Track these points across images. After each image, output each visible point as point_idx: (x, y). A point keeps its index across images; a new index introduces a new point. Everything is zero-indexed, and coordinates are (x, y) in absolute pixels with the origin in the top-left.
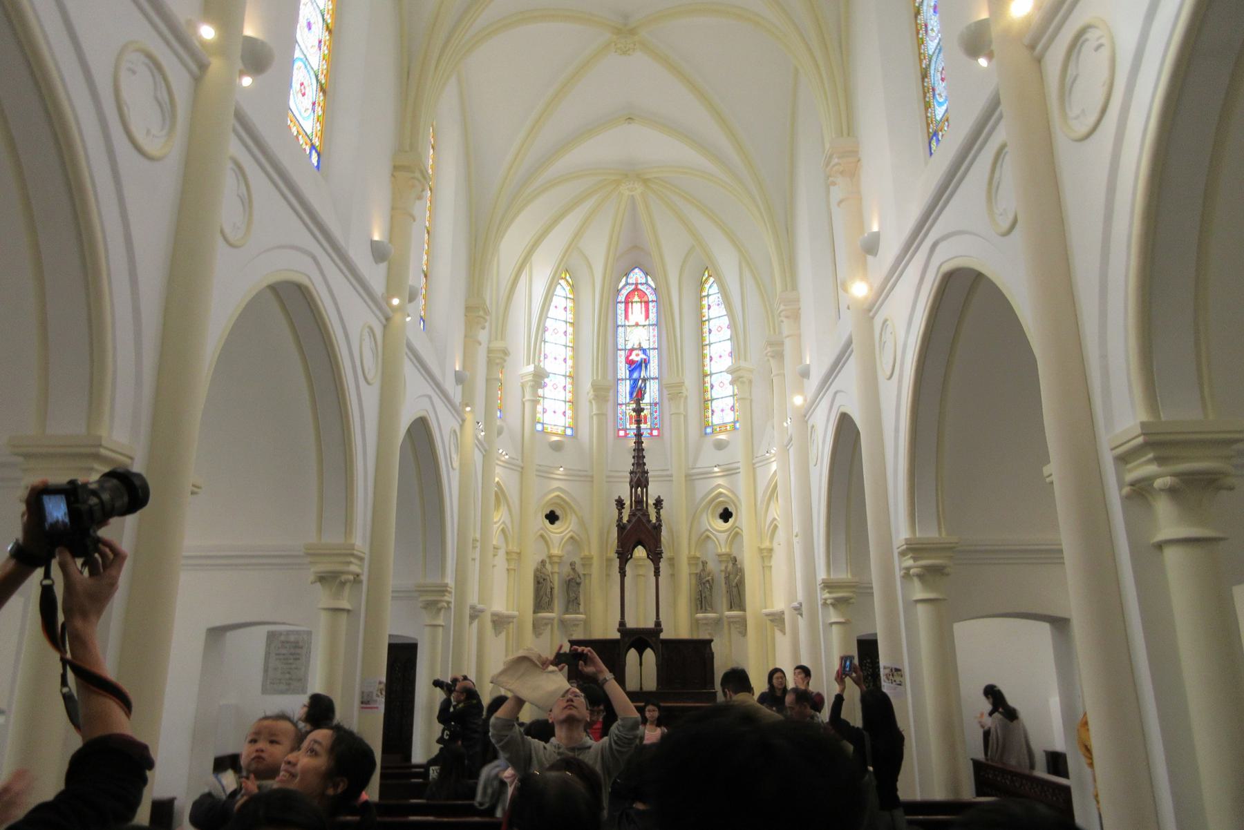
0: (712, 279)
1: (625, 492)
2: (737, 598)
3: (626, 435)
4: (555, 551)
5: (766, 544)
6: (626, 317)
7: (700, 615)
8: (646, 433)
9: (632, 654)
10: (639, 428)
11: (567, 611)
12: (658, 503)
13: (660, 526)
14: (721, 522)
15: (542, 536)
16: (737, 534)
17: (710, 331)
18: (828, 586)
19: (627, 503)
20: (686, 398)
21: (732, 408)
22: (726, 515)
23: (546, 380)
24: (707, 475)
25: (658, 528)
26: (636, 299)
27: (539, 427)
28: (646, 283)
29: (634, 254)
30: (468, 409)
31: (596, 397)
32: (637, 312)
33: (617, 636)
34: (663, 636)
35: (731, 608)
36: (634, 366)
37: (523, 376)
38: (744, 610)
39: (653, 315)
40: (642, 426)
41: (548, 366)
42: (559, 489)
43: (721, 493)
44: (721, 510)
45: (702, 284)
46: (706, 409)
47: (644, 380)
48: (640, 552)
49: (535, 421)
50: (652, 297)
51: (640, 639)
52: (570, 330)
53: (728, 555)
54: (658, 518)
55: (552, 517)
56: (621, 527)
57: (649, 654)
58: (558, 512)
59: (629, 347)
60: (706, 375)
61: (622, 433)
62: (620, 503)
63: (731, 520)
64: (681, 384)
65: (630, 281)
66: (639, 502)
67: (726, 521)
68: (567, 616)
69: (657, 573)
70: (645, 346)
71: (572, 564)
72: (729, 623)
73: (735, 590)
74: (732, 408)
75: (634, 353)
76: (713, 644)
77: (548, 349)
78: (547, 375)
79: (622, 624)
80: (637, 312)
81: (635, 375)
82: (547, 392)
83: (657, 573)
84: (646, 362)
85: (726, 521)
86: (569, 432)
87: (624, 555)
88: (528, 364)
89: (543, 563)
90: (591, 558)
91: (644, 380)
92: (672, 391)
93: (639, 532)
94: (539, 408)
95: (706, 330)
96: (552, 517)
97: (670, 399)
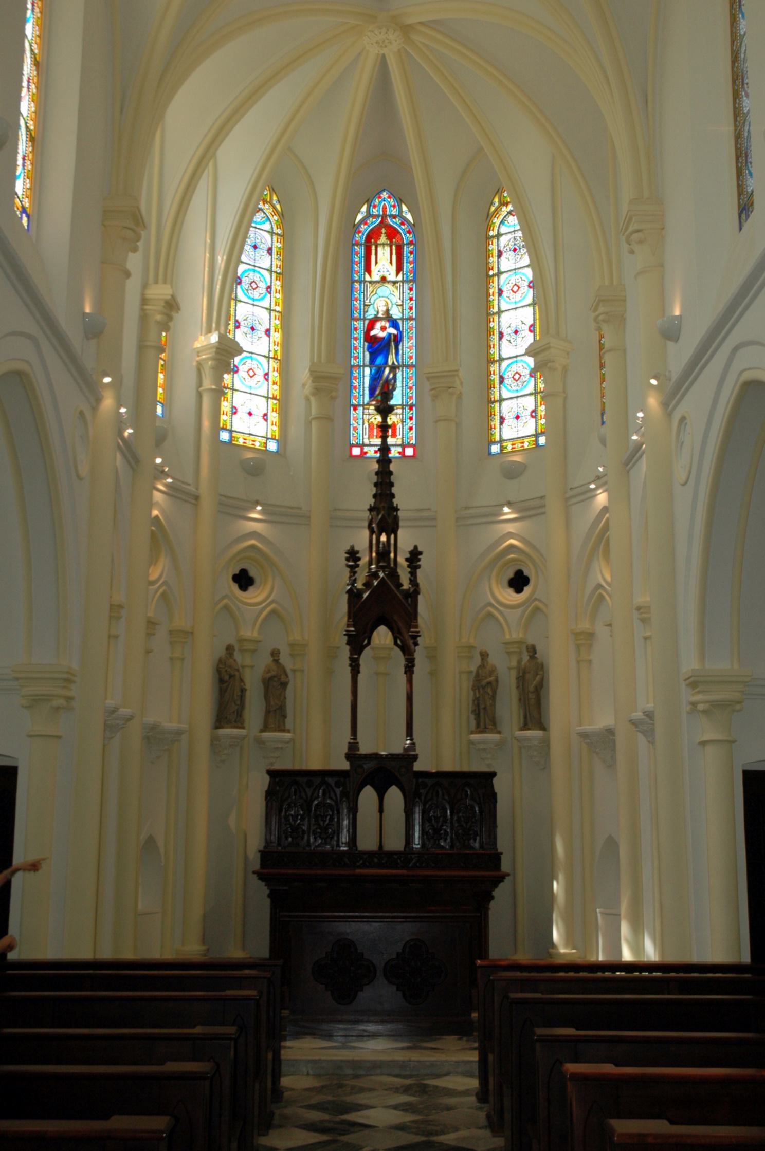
0: (505, 210)
1: (361, 539)
2: (534, 712)
3: (363, 453)
4: (248, 633)
5: (585, 625)
6: (368, 269)
7: (475, 737)
8: (394, 453)
9: (368, 795)
10: (384, 438)
11: (265, 728)
12: (414, 557)
13: (417, 592)
14: (511, 591)
15: (226, 608)
16: (537, 609)
17: (500, 292)
18: (694, 683)
19: (365, 559)
20: (460, 397)
21: (534, 414)
22: (519, 582)
23: (237, 360)
24: (492, 515)
25: (414, 594)
26: (383, 239)
27: (224, 436)
28: (400, 215)
29: (380, 165)
30: (107, 380)
31: (317, 391)
32: (384, 262)
33: (345, 765)
34: (418, 766)
35: (525, 727)
36: (378, 348)
37: (199, 352)
38: (543, 728)
39: (407, 266)
40: (390, 441)
41: (241, 337)
43: (512, 546)
44: (510, 574)
45: (489, 217)
46: (490, 415)
47: (393, 368)
48: (382, 636)
49: (217, 428)
50: (407, 238)
51: (384, 771)
52: (277, 285)
53: (520, 643)
54: (414, 581)
55: (244, 580)
56: (353, 595)
57: (394, 795)
58: (252, 573)
59: (371, 314)
60: (493, 362)
61: (356, 451)
62: (353, 555)
63: (527, 590)
64: (454, 374)
65: (375, 211)
66: (383, 555)
67: (519, 590)
68: (266, 735)
69: (409, 668)
70: (396, 313)
71: (275, 654)
72: (520, 748)
73: (532, 696)
74: (534, 414)
75: (378, 325)
76: (495, 780)
77: (242, 311)
78: (240, 351)
79: (353, 746)
80: (384, 262)
81: (379, 360)
82: (239, 381)
83: (409, 668)
84: (398, 339)
85: (519, 590)
86: (272, 446)
87: (358, 642)
88: (209, 331)
89: (230, 649)
92: (437, 384)
93: (383, 604)
94: (225, 406)
95: (494, 290)
96: (244, 580)
97: (435, 397)
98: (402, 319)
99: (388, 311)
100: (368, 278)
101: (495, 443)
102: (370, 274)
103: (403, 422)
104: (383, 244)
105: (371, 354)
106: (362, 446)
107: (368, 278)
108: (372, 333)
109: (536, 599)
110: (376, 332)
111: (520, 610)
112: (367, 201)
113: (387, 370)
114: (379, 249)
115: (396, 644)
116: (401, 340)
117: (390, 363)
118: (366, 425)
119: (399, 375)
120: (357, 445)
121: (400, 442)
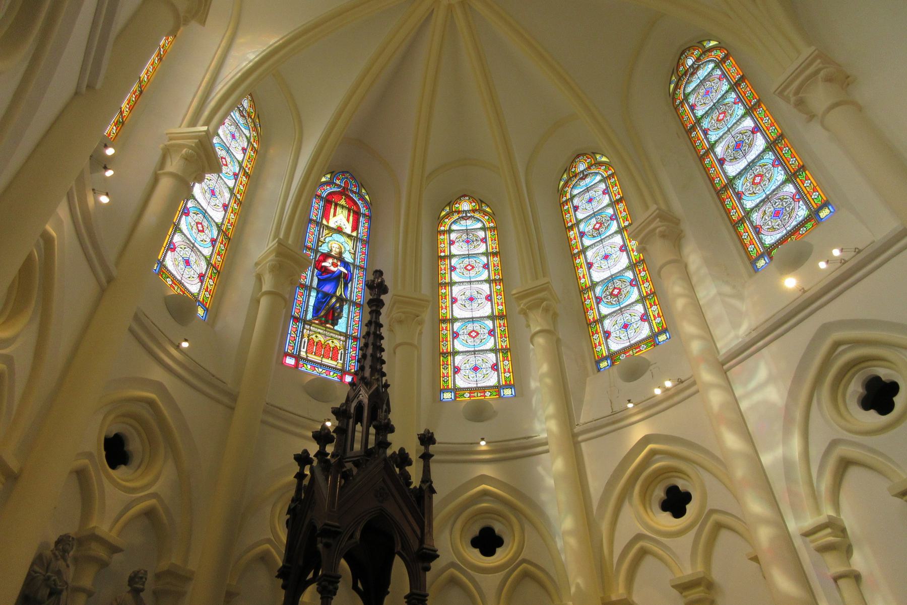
6: (326, 215)
42: (160, 387)
43: (485, 493)
44: (475, 531)
50: (363, 210)
58: (134, 445)
61: (290, 361)
75: (330, 261)
81: (327, 288)
90: (185, 578)
91: (341, 300)
98: (353, 264)
99: (340, 253)
100: (324, 222)
101: (447, 390)
102: (328, 220)
103: (345, 349)
104: (343, 207)
105: (319, 279)
106: (298, 358)
107: (324, 222)
108: (323, 264)
109: (524, 561)
110: (328, 264)
111: (500, 575)
112: (332, 173)
113: (334, 300)
114: (339, 210)
115: (355, 587)
116: (351, 280)
117: (338, 294)
118: (306, 339)
119: (346, 307)
120: (291, 356)
121: (339, 366)
